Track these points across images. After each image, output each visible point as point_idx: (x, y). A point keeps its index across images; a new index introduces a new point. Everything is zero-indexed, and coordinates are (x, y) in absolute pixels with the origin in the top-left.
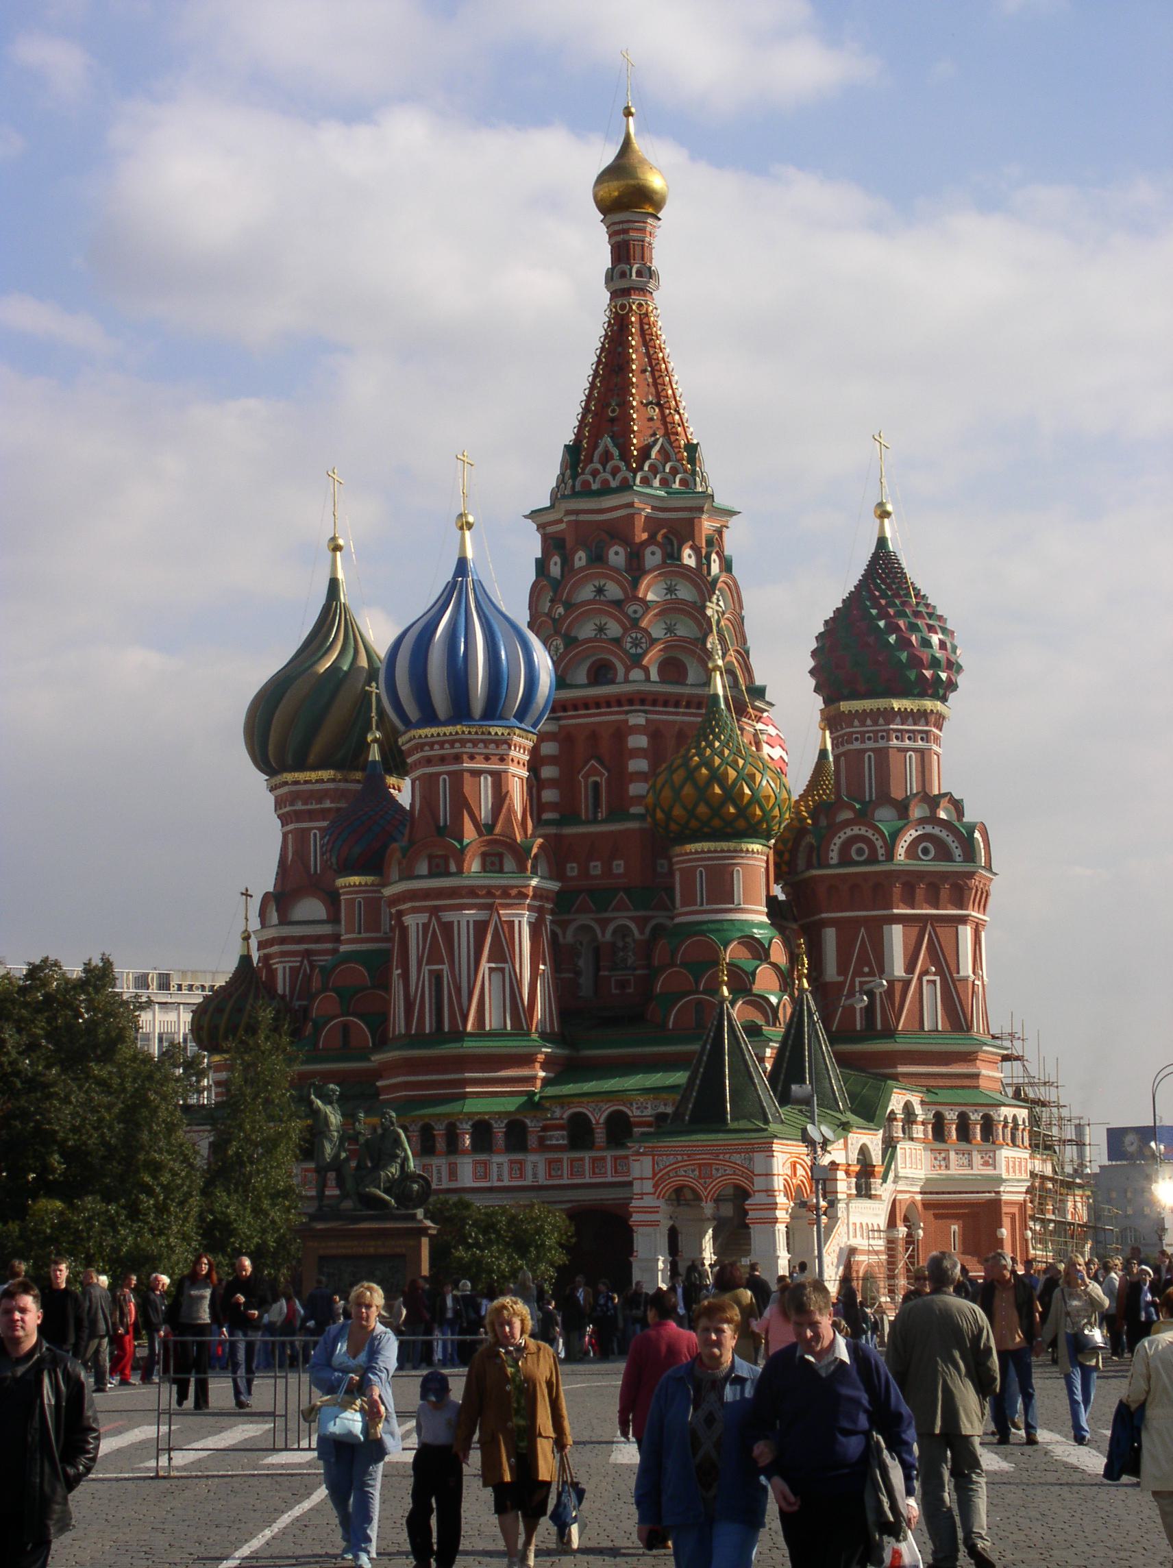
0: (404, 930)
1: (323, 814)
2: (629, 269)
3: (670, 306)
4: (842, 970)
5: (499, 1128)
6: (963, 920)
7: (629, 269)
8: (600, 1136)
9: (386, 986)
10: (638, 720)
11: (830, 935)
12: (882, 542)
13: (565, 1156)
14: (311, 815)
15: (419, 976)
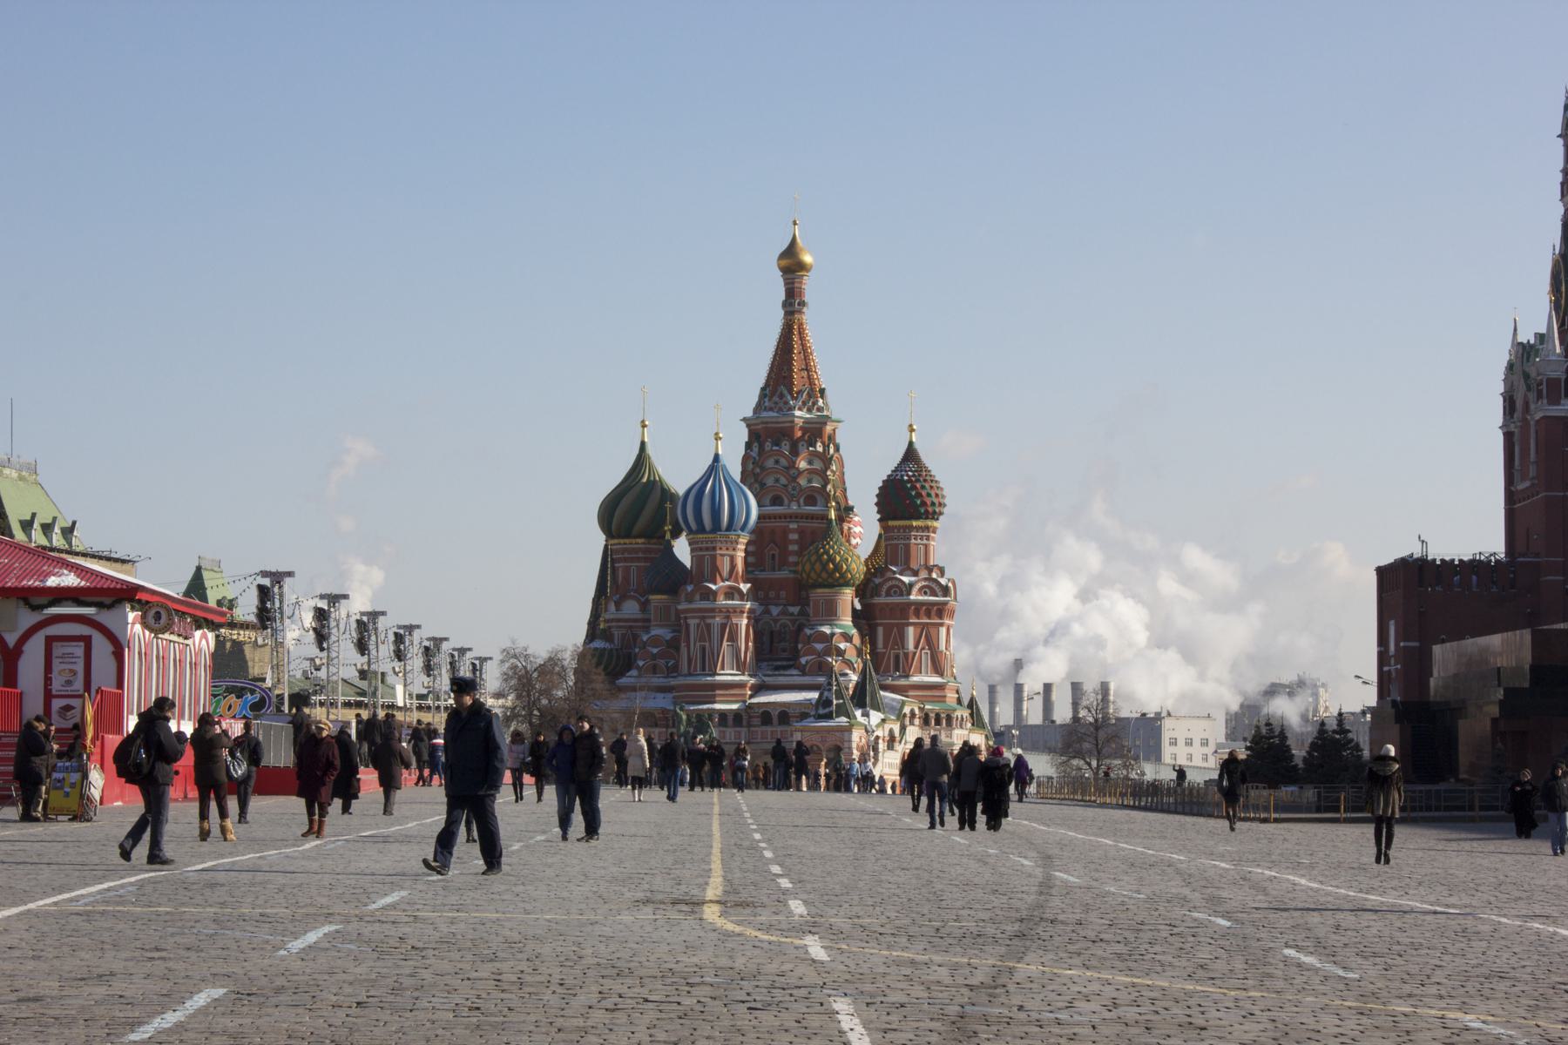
0: (688, 626)
1: (638, 559)
2: (793, 301)
3: (812, 320)
4: (885, 646)
5: (730, 718)
6: (942, 625)
7: (793, 301)
8: (775, 720)
9: (678, 649)
10: (793, 526)
11: (880, 630)
12: (911, 443)
13: (759, 729)
14: (633, 560)
15: (695, 647)
